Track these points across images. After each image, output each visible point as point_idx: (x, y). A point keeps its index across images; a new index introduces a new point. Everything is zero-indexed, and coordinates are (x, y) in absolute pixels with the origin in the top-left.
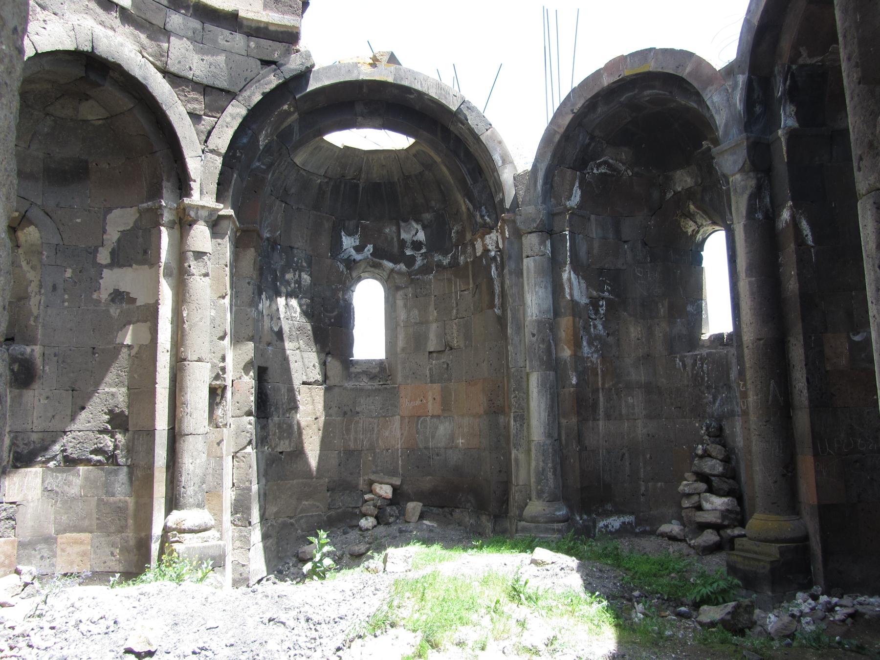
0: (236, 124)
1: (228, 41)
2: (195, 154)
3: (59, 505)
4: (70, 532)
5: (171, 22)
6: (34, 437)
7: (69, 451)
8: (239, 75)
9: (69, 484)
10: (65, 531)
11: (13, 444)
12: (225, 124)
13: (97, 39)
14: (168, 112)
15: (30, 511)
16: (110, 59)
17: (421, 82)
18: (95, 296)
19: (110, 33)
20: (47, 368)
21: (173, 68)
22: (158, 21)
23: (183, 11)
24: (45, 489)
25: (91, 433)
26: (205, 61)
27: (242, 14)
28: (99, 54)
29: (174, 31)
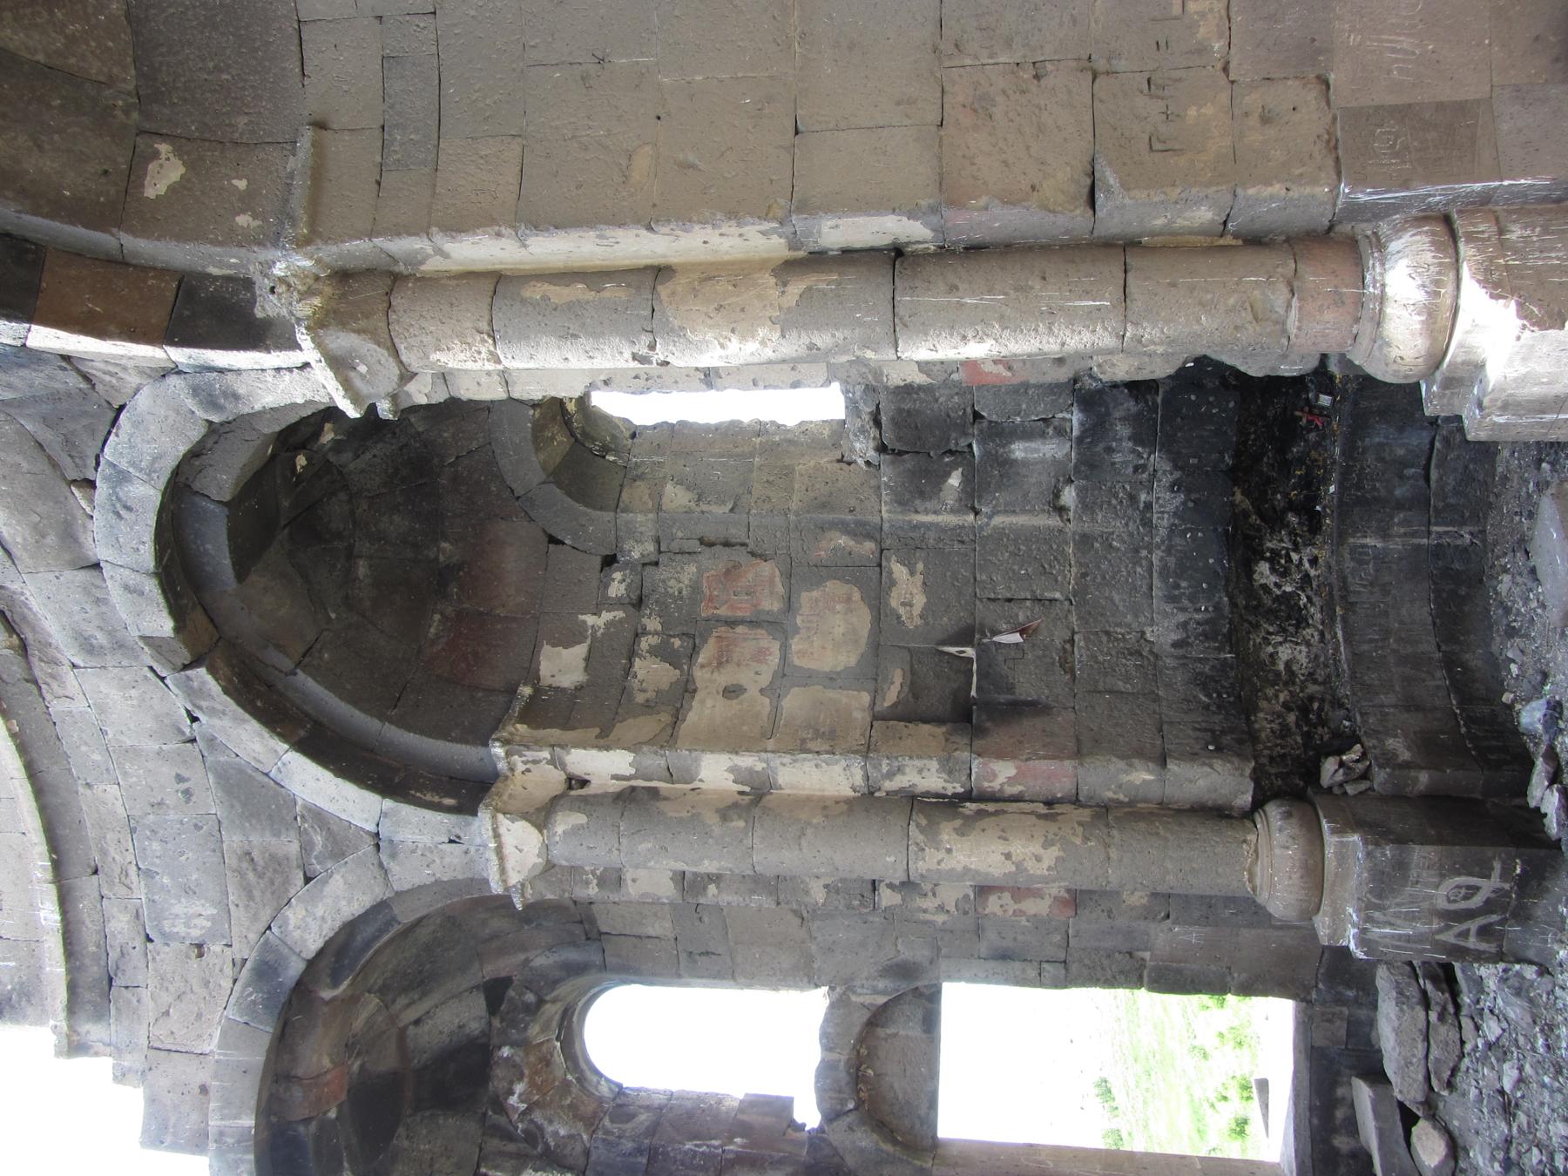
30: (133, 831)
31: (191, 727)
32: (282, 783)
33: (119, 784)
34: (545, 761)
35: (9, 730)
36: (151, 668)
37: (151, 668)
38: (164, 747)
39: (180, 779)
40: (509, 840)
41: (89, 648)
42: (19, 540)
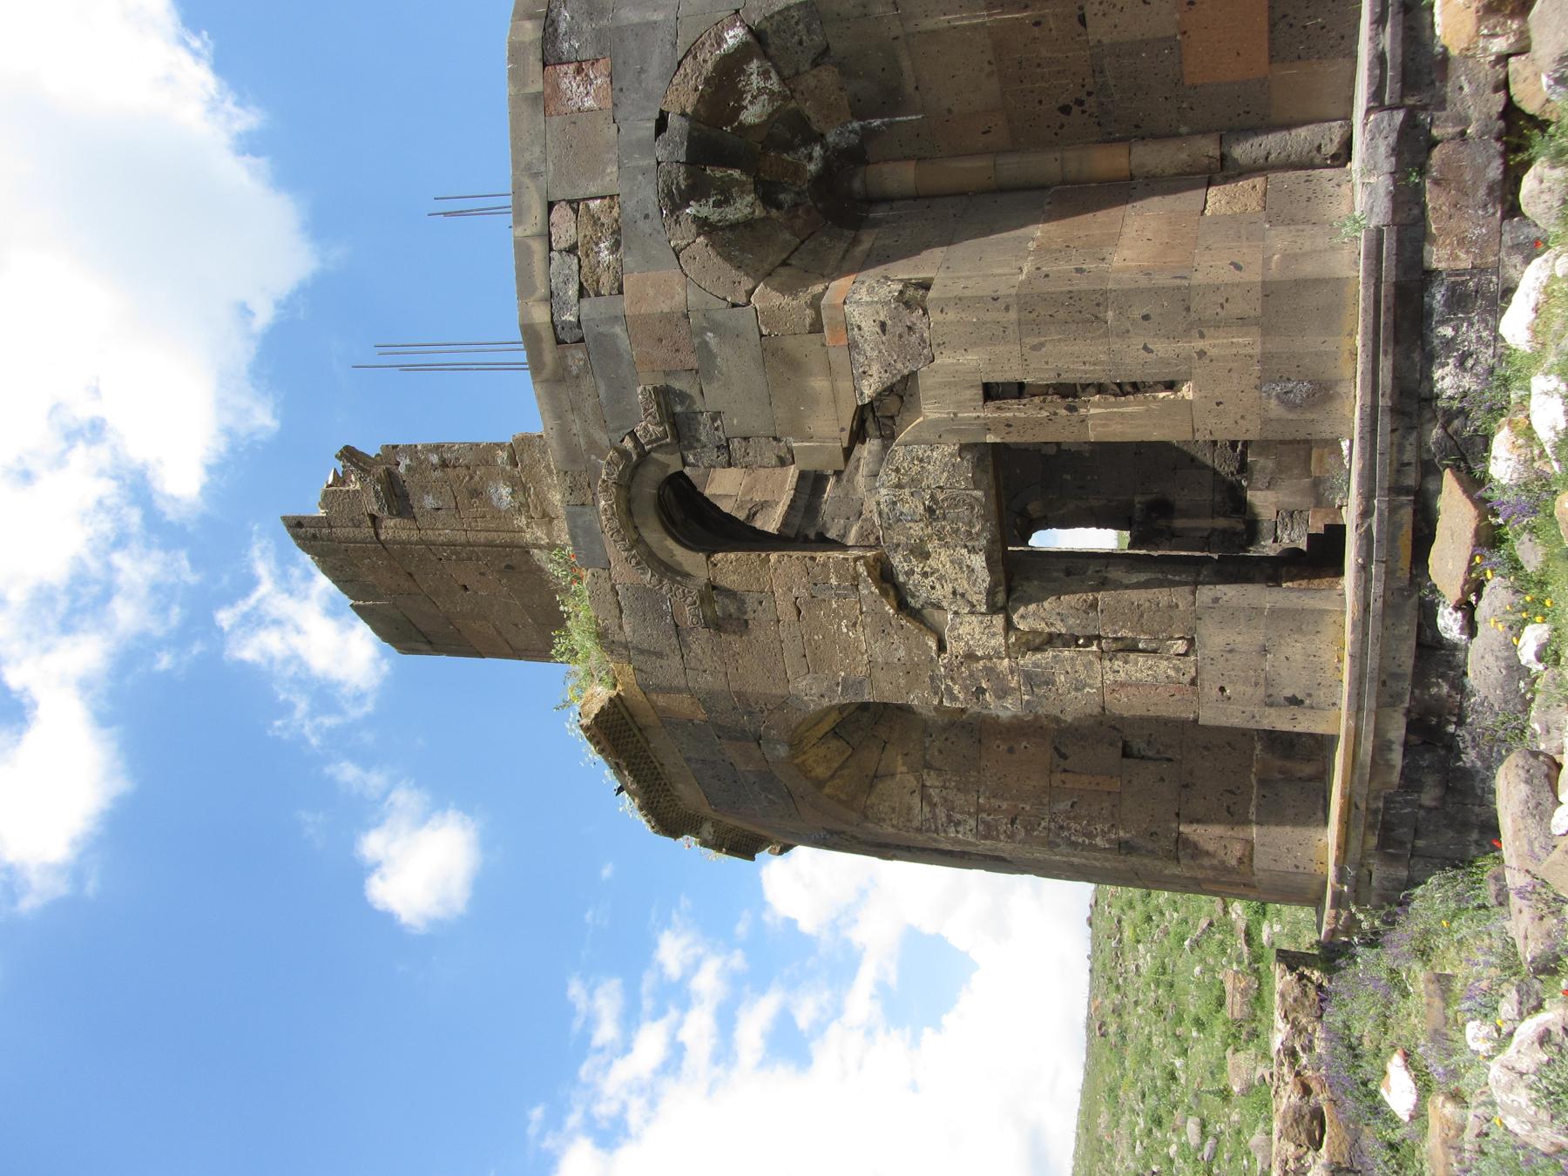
3: (1283, 476)
4: (1310, 465)
6: (1218, 498)
7: (1232, 469)
9: (1263, 468)
10: (1309, 471)
11: (1225, 515)
15: (1286, 499)
18: (1087, 455)
19: (862, 462)
20: (1155, 490)
24: (1268, 488)
25: (1217, 451)
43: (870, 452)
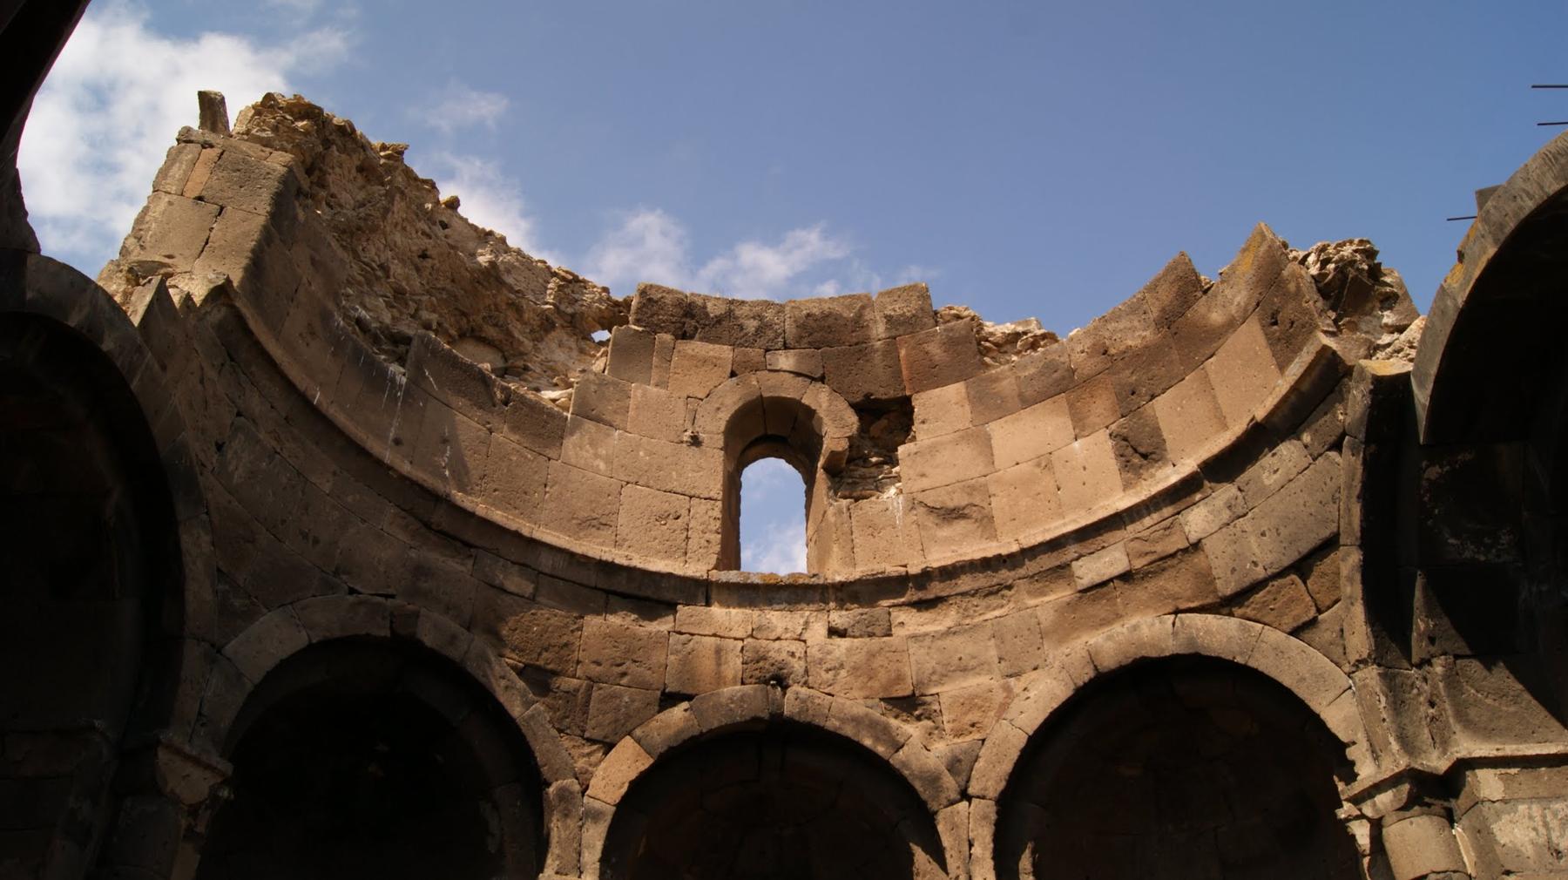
0: (1357, 590)
1: (1278, 470)
2: (1331, 695)
5: (1194, 528)
8: (1321, 502)
12: (1349, 601)
13: (1097, 653)
14: (1252, 664)
16: (1125, 662)
17: (1524, 190)
21: (1227, 586)
22: (1175, 543)
23: (1198, 496)
26: (1267, 533)
27: (1260, 414)
28: (1106, 670)
29: (1203, 535)
30: (299, 474)
31: (346, 583)
32: (281, 609)
33: (328, 495)
34: (193, 823)
35: (395, 471)
36: (392, 596)
37: (392, 596)
38: (339, 551)
39: (316, 541)
40: (196, 773)
41: (420, 571)
42: (499, 602)
43: (1135, 628)
